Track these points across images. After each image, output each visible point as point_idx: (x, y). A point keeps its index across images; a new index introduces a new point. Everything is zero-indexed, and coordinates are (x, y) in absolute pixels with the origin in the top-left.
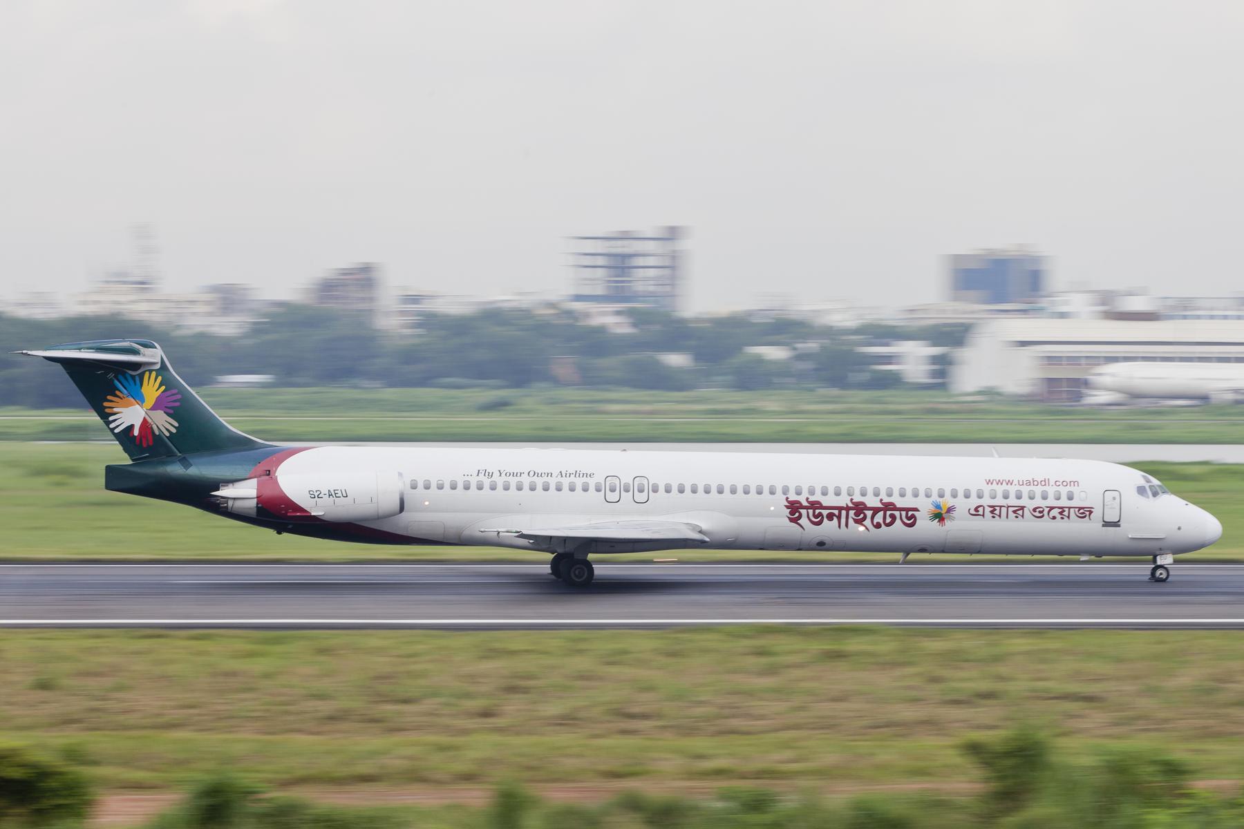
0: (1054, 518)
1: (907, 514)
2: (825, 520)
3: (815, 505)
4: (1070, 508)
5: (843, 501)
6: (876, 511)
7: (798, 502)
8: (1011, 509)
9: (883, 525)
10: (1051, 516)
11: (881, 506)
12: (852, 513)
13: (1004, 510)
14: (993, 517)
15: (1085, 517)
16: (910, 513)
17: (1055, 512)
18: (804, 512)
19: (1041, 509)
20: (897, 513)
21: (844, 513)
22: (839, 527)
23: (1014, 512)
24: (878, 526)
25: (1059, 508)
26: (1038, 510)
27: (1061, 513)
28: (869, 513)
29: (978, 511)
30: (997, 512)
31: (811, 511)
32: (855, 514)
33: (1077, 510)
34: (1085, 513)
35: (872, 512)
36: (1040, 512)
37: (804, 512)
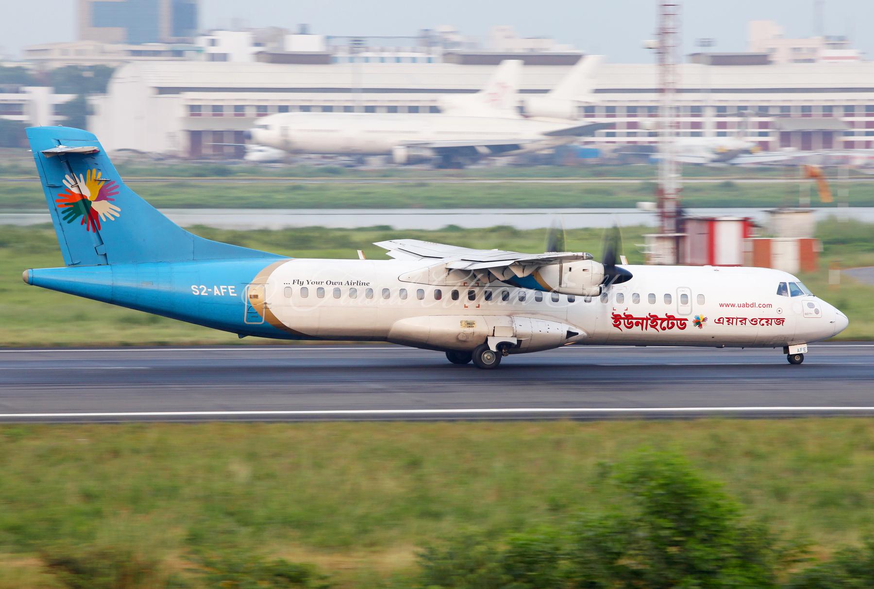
0: (763, 325)
1: (681, 322)
2: (634, 325)
3: (629, 317)
4: (772, 319)
6: (663, 320)
8: (739, 320)
9: (667, 329)
10: (761, 324)
12: (649, 322)
13: (735, 320)
14: (729, 324)
15: (780, 324)
17: (763, 322)
18: (622, 321)
20: (675, 322)
21: (645, 321)
22: (642, 329)
23: (741, 321)
24: (664, 329)
25: (766, 319)
27: (767, 322)
28: (659, 322)
30: (731, 321)
31: (626, 321)
32: (652, 322)
33: (776, 320)
34: (780, 321)
36: (755, 321)
37: (622, 321)
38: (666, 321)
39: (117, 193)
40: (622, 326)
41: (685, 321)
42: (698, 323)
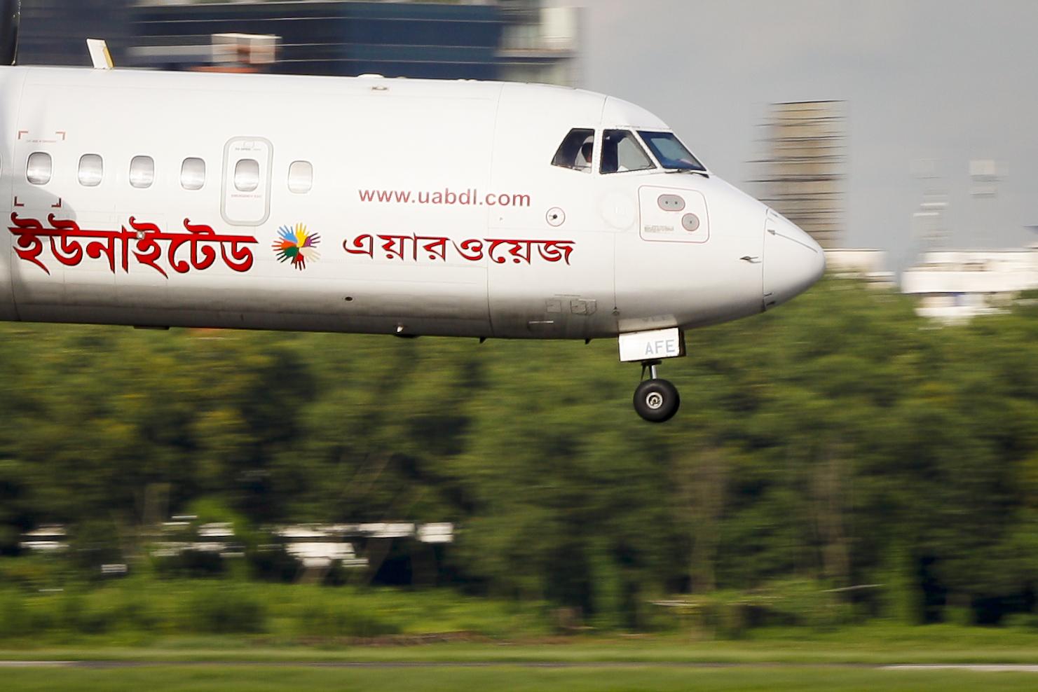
0: (502, 260)
4: (529, 243)
6: (177, 240)
7: (35, 222)
8: (421, 243)
10: (496, 257)
11: (186, 232)
12: (132, 244)
13: (408, 244)
19: (477, 245)
20: (216, 246)
21: (118, 243)
22: (113, 268)
23: (428, 248)
24: (183, 268)
26: (471, 245)
27: (513, 252)
28: (165, 245)
29: (361, 245)
31: (58, 240)
32: (139, 246)
34: (559, 250)
35: (169, 242)
36: (475, 249)
37: (46, 242)
38: (188, 244)
40: (46, 256)
41: (249, 246)
42: (292, 252)
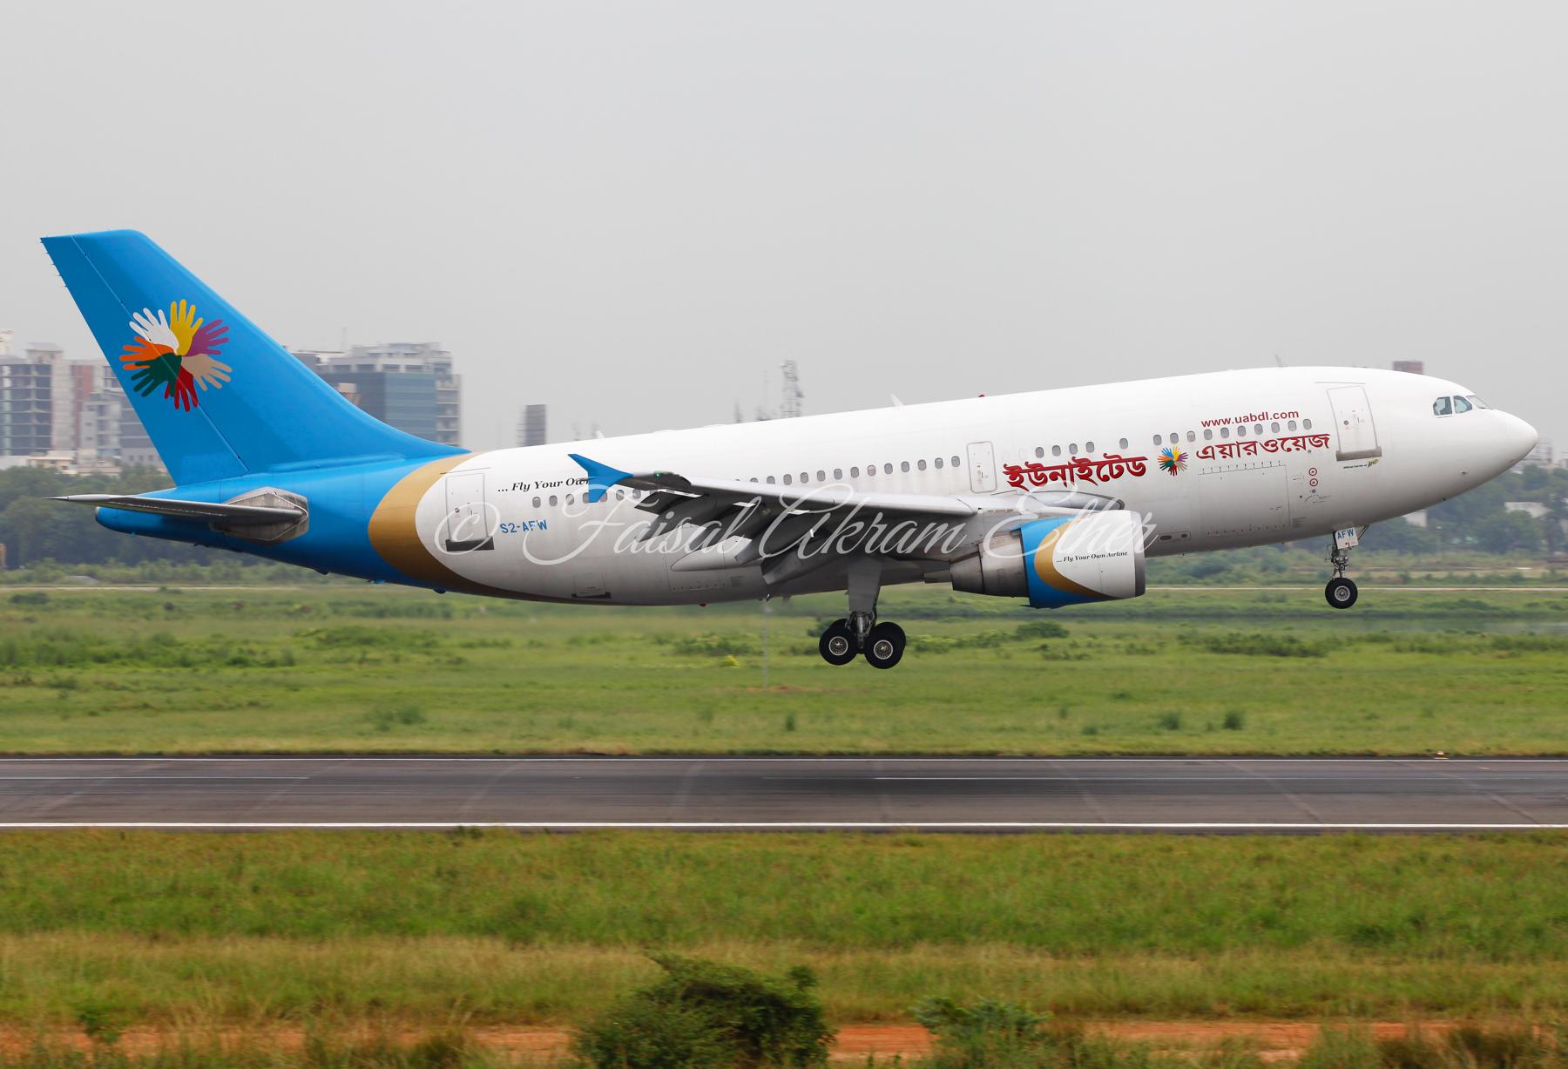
0: (1289, 450)
3: (1035, 468)
5: (1065, 459)
6: (1100, 465)
8: (1241, 447)
12: (1076, 470)
13: (1234, 448)
14: (1224, 457)
16: (1137, 463)
17: (1289, 444)
18: (1025, 475)
20: (1124, 465)
21: (1067, 471)
23: (1245, 449)
24: (1106, 479)
25: (1292, 439)
26: (1270, 444)
28: (1094, 468)
31: (1032, 474)
36: (1273, 446)
38: (1107, 466)
39: (226, 340)
